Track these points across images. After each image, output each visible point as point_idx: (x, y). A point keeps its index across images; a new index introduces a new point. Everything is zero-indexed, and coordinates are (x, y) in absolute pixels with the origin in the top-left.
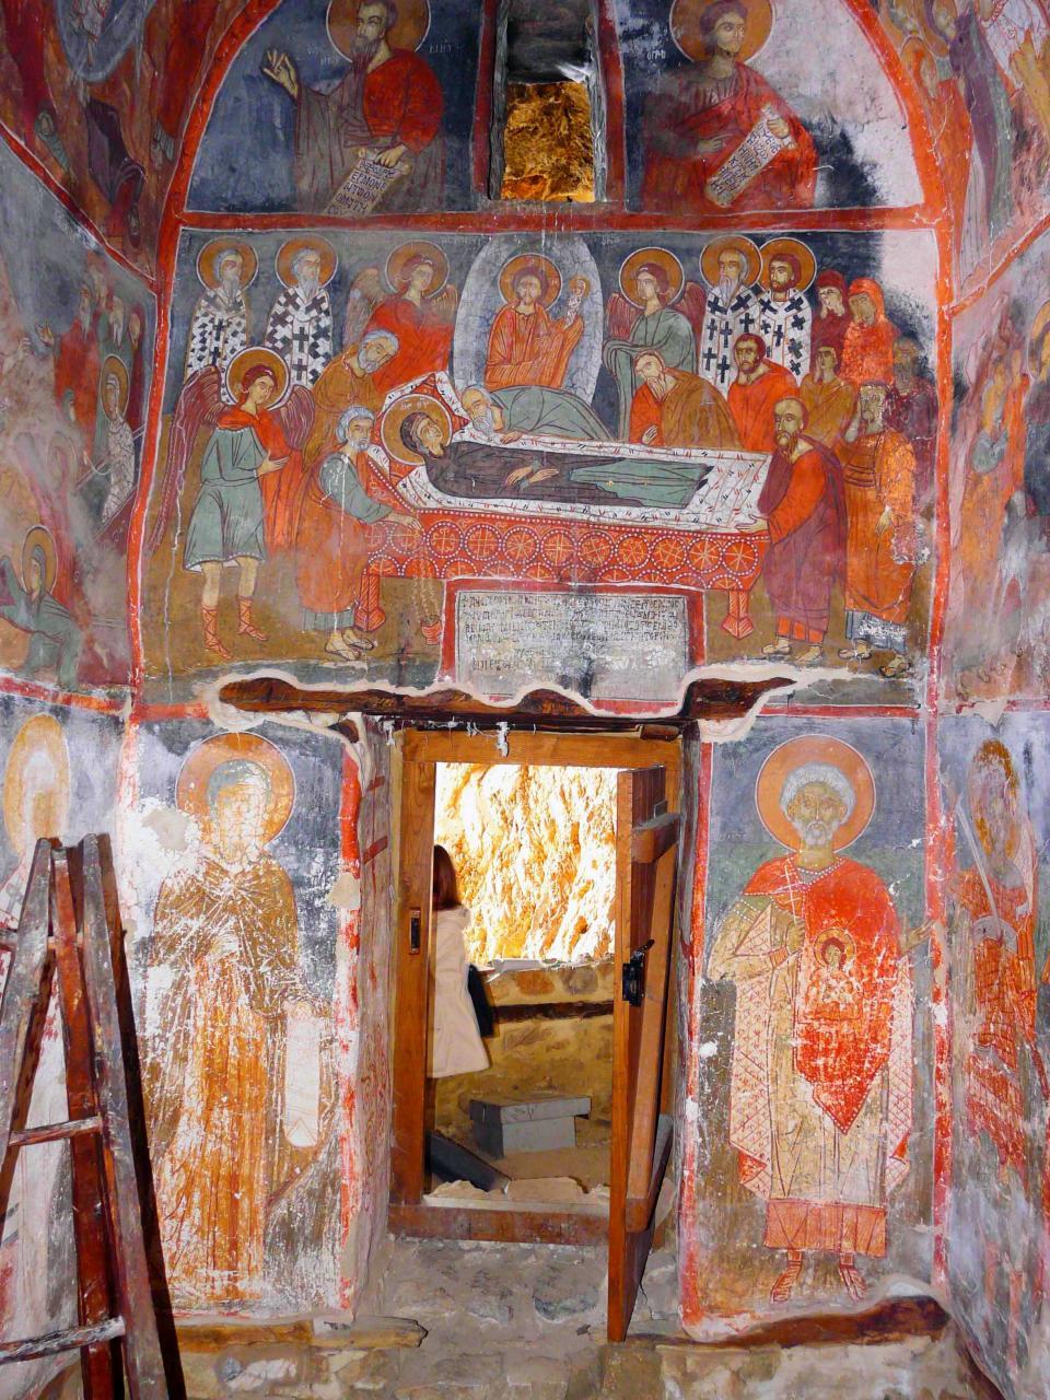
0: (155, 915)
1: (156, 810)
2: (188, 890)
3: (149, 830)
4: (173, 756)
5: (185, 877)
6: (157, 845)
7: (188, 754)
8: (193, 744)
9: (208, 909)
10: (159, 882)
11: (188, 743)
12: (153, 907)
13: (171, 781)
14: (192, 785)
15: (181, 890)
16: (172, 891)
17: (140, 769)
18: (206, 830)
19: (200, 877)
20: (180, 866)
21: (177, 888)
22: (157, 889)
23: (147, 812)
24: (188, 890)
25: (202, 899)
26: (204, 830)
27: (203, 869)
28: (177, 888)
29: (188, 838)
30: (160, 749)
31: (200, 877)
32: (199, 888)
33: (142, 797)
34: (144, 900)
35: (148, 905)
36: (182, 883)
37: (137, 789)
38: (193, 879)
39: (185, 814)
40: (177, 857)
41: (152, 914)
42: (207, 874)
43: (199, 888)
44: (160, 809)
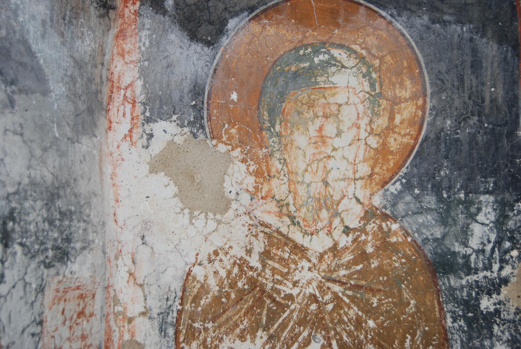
0: (177, 333)
1: (171, 143)
2: (233, 285)
3: (161, 178)
4: (197, 47)
5: (227, 262)
6: (177, 203)
7: (225, 41)
8: (232, 23)
9: (271, 320)
10: (181, 273)
11: (224, 23)
12: (172, 317)
13: (197, 91)
14: (234, 96)
15: (221, 285)
16: (204, 289)
17: (143, 73)
18: (262, 174)
19: (254, 261)
20: (218, 241)
21: (212, 282)
22: (177, 286)
23: (157, 146)
24: (233, 285)
25: (259, 302)
26: (258, 174)
27: (259, 246)
28: (212, 282)
29: (229, 186)
30: (176, 39)
31: (254, 261)
32: (253, 283)
33: (148, 120)
34: (156, 306)
35: (164, 314)
36: (223, 273)
37: (139, 109)
38: (242, 264)
39: (222, 148)
40: (212, 225)
41: (171, 331)
42: (266, 255)
43: (253, 283)
44: (179, 140)
